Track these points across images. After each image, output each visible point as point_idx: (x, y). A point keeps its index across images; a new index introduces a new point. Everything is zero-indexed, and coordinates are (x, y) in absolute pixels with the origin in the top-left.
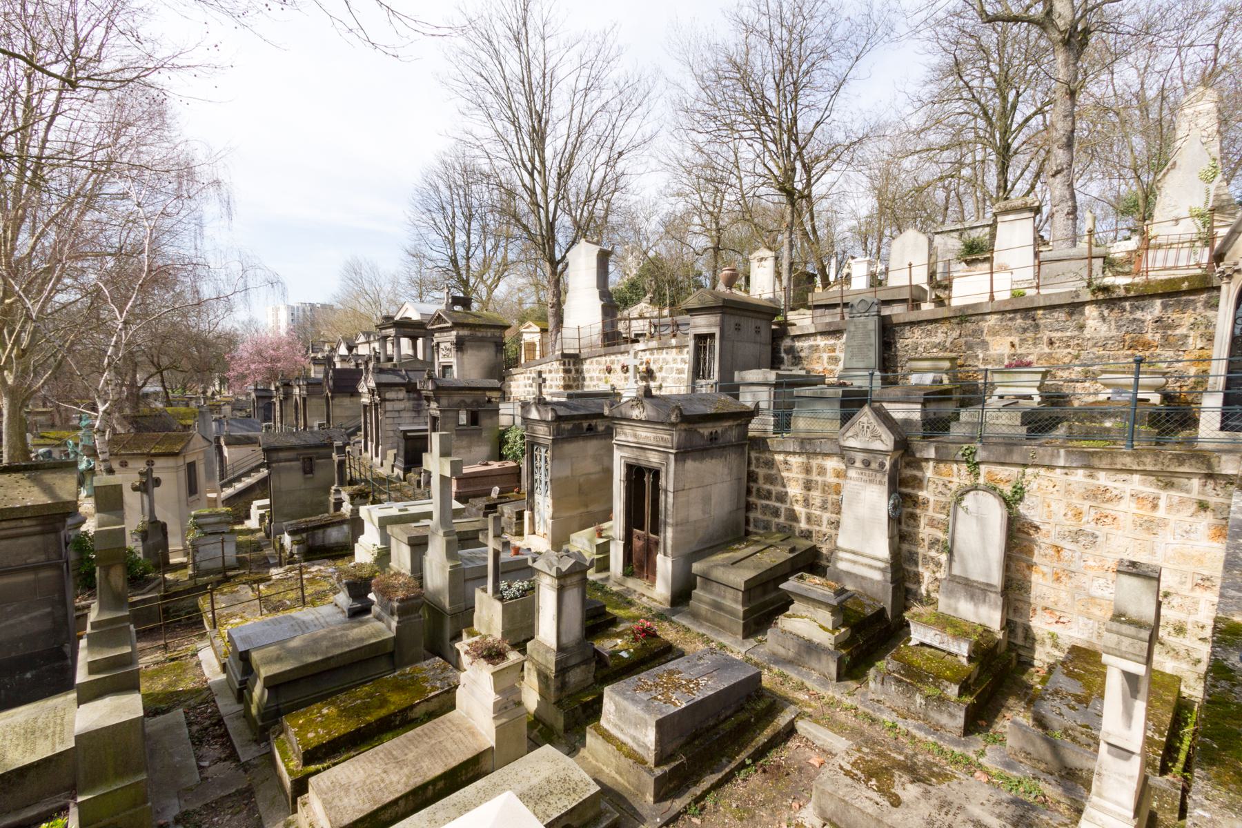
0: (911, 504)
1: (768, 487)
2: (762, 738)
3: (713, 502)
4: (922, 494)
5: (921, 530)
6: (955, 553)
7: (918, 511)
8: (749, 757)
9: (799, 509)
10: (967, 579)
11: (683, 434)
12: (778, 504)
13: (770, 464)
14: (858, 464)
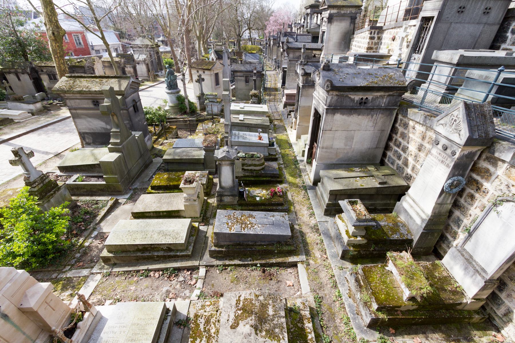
0: (475, 188)
1: (400, 140)
2: (274, 261)
3: (354, 141)
4: (486, 185)
5: (472, 209)
6: (474, 236)
7: (477, 195)
8: (260, 264)
9: (411, 161)
10: (471, 257)
11: (335, 98)
12: (402, 153)
13: (406, 126)
14: (440, 146)
